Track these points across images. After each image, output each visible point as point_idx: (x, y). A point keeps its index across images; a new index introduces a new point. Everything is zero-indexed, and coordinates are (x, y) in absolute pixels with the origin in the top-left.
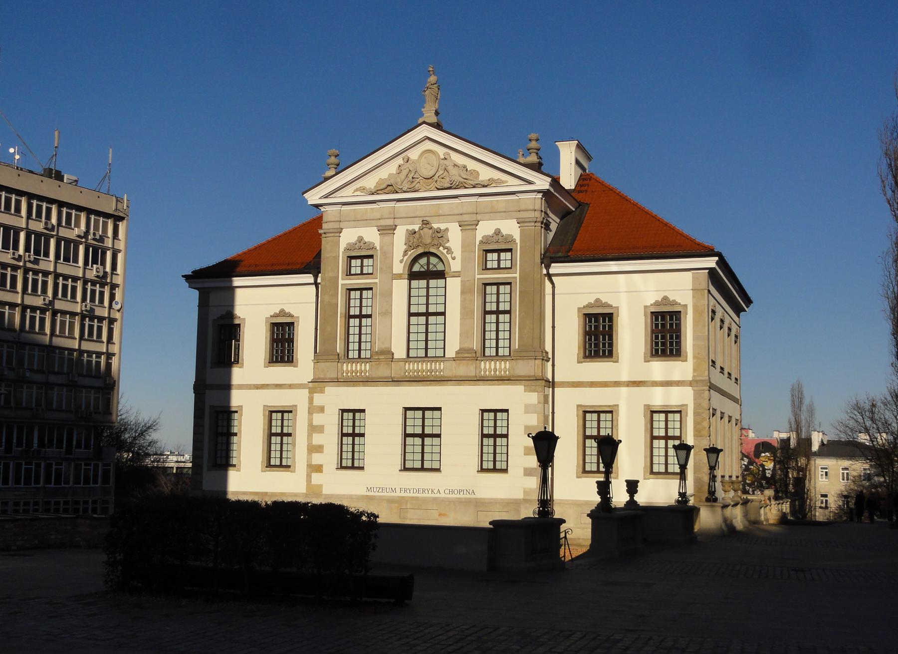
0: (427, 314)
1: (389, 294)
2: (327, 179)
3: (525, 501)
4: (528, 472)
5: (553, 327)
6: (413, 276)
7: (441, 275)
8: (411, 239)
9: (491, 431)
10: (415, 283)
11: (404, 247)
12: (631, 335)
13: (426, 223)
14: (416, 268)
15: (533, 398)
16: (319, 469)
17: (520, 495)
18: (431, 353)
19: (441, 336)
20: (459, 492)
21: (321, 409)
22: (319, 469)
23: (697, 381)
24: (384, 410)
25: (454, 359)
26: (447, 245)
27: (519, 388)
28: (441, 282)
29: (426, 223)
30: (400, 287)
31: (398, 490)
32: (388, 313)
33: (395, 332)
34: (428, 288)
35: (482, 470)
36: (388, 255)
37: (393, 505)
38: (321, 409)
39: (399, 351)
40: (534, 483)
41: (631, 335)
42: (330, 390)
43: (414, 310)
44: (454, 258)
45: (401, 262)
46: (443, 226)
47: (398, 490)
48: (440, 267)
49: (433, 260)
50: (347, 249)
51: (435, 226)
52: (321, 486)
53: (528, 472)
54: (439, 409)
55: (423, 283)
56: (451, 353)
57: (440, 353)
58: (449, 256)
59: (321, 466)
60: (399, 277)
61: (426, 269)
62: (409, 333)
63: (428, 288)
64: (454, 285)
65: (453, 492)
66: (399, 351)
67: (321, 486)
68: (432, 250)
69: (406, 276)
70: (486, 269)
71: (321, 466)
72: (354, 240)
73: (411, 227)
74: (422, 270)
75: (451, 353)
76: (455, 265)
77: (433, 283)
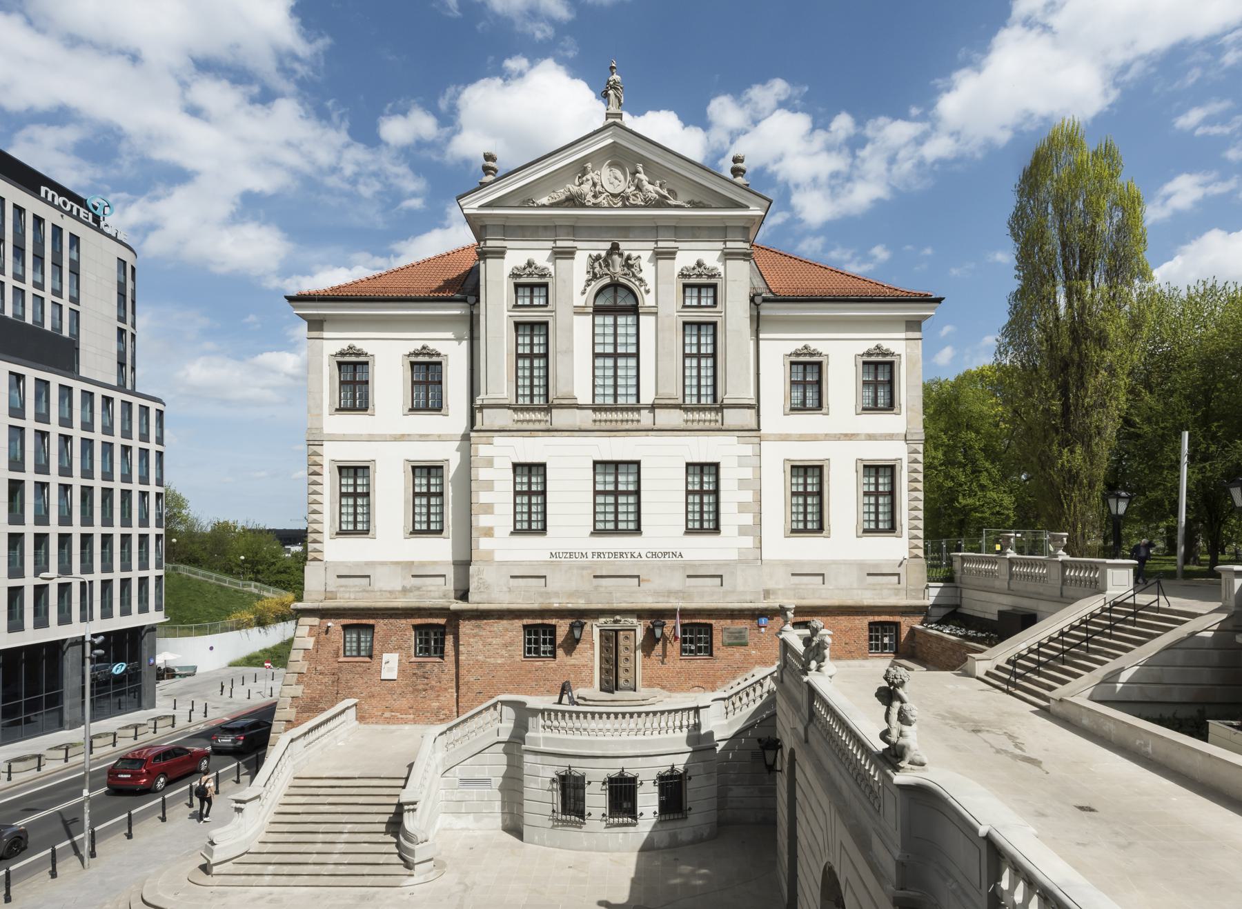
0: (615, 356)
1: (571, 330)
2: (483, 185)
3: (740, 561)
4: (743, 530)
5: (758, 374)
6: (598, 311)
7: (634, 310)
8: (597, 264)
9: (697, 488)
10: (599, 320)
11: (587, 277)
12: (842, 381)
13: (615, 248)
14: (600, 302)
15: (748, 450)
16: (489, 532)
17: (734, 556)
18: (621, 400)
19: (633, 382)
20: (665, 554)
21: (489, 462)
22: (489, 532)
23: (912, 434)
24: (570, 462)
25: (653, 408)
26: (640, 275)
27: (731, 439)
28: (631, 320)
29: (615, 248)
30: (583, 325)
31: (590, 555)
32: (570, 351)
33: (576, 373)
34: (615, 325)
35: (689, 531)
36: (569, 282)
37: (585, 572)
38: (489, 462)
39: (585, 397)
40: (748, 542)
41: (842, 381)
42: (498, 440)
43: (599, 350)
44: (648, 292)
45: (583, 293)
46: (634, 254)
47: (590, 555)
48: (630, 302)
49: (622, 293)
50: (514, 275)
51: (626, 253)
52: (491, 552)
53: (743, 530)
54: (638, 463)
55: (609, 320)
56: (647, 397)
57: (632, 400)
58: (642, 289)
59: (491, 529)
60: (579, 311)
61: (617, 300)
62: (594, 376)
63: (615, 325)
64: (647, 322)
65: (655, 555)
66: (585, 397)
67: (491, 552)
68: (622, 280)
69: (591, 310)
70: (684, 306)
71: (491, 529)
72: (523, 264)
73: (595, 253)
74: (608, 303)
75: (647, 397)
76: (647, 300)
77: (621, 320)
